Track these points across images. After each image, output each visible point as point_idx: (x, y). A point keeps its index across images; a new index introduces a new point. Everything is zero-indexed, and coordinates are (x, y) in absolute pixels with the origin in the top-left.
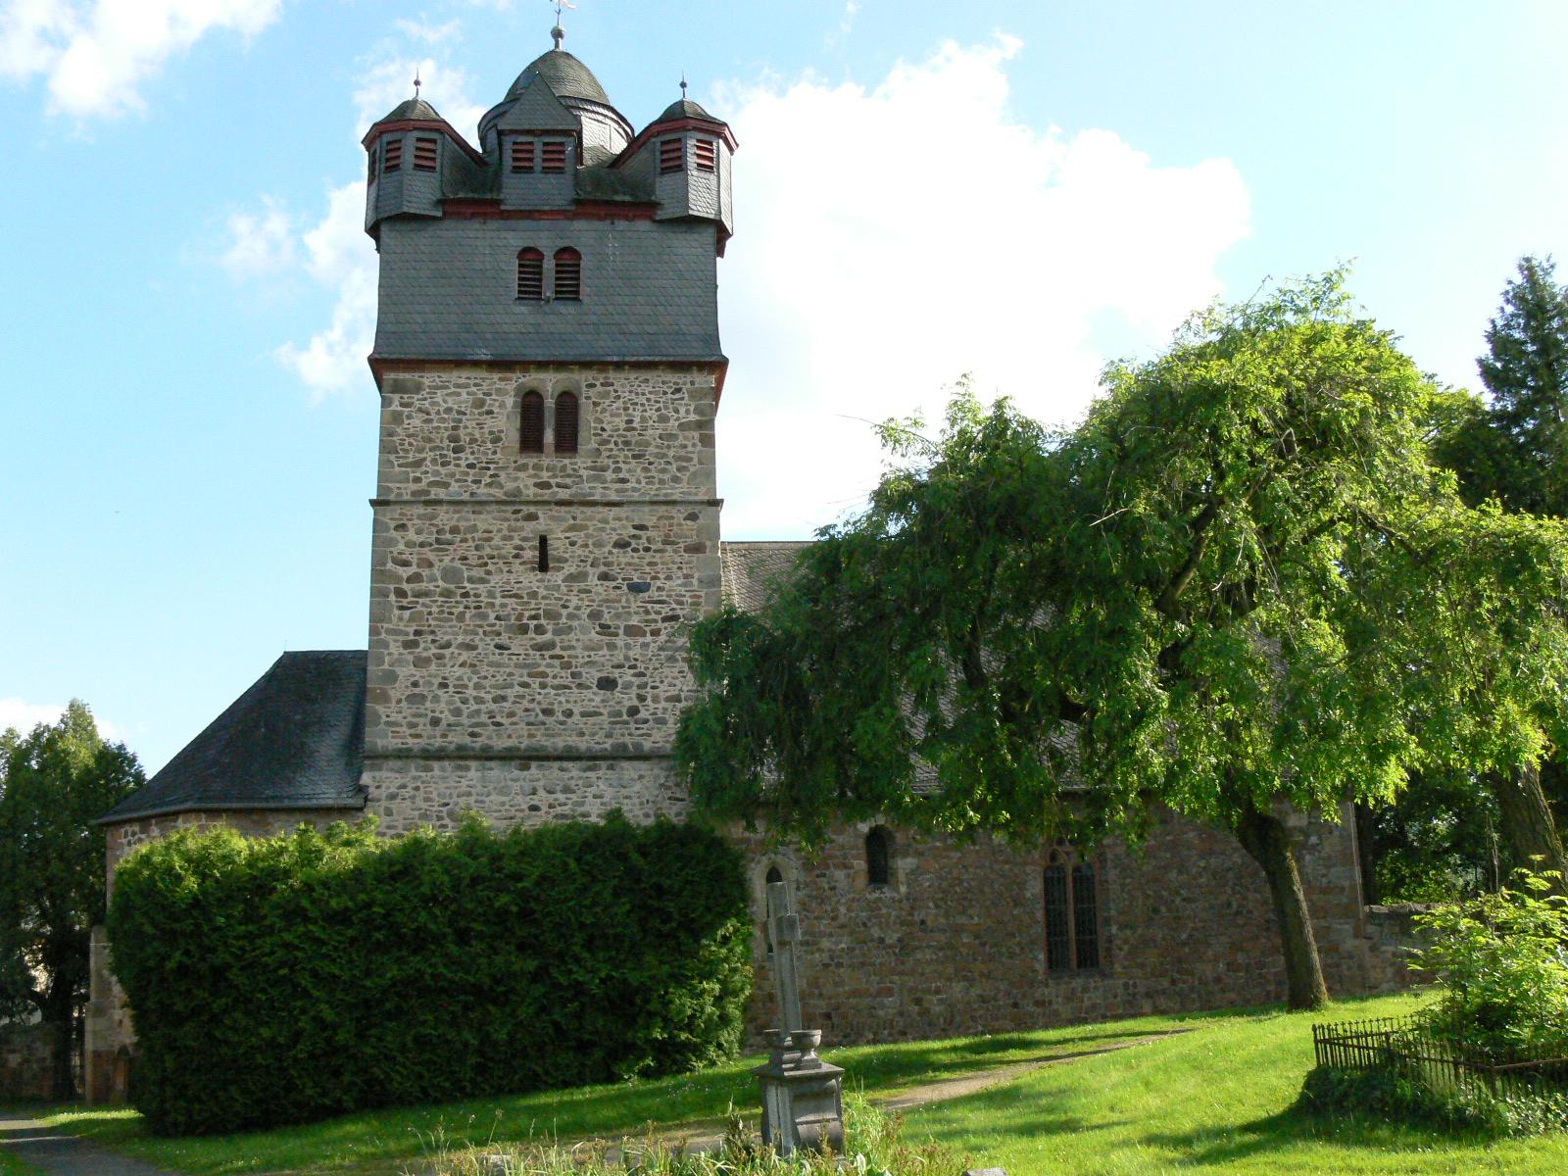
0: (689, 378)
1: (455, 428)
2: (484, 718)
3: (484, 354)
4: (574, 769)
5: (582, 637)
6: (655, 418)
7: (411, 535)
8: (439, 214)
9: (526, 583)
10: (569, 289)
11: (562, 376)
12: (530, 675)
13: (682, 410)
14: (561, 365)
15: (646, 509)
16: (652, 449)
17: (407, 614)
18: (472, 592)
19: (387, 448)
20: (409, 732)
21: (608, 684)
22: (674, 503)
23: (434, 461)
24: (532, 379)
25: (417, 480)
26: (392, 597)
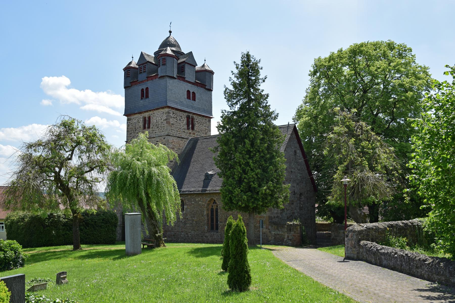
11: (148, 113)
14: (147, 111)
19: (128, 131)
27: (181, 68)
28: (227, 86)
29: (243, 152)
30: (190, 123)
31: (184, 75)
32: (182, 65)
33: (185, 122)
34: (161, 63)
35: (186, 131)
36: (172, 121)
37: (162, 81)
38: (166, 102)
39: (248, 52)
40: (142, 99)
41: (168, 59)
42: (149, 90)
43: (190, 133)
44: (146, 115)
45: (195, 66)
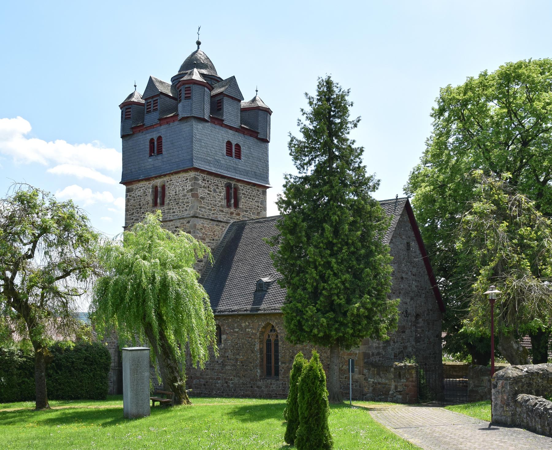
3: (142, 177)
11: (162, 180)
13: (188, 186)
14: (160, 177)
15: (178, 221)
16: (181, 201)
19: (127, 210)
27: (217, 104)
28: (293, 135)
29: (321, 245)
30: (232, 196)
31: (222, 115)
32: (218, 98)
33: (223, 194)
34: (183, 96)
35: (225, 210)
36: (201, 192)
37: (185, 127)
38: (191, 160)
39: (329, 77)
40: (151, 155)
41: (195, 88)
42: (163, 141)
43: (232, 213)
44: (158, 182)
45: (240, 101)
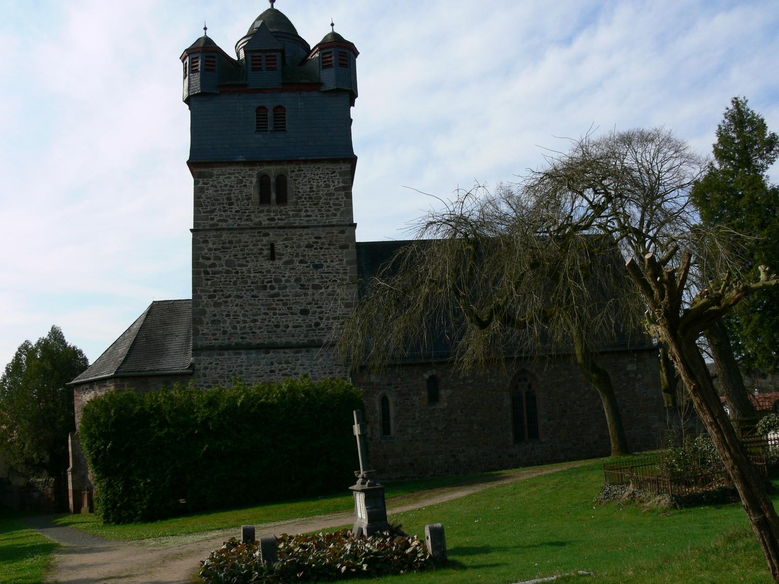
0: (339, 166)
1: (229, 194)
2: (247, 330)
3: (241, 158)
4: (290, 353)
5: (292, 290)
6: (323, 186)
7: (210, 245)
8: (218, 92)
9: (265, 267)
10: (279, 126)
12: (268, 309)
13: (336, 183)
15: (321, 229)
17: (209, 282)
18: (240, 271)
20: (212, 338)
21: (305, 312)
22: (333, 226)
23: (220, 210)
24: (265, 169)
25: (212, 219)
26: (203, 275)
